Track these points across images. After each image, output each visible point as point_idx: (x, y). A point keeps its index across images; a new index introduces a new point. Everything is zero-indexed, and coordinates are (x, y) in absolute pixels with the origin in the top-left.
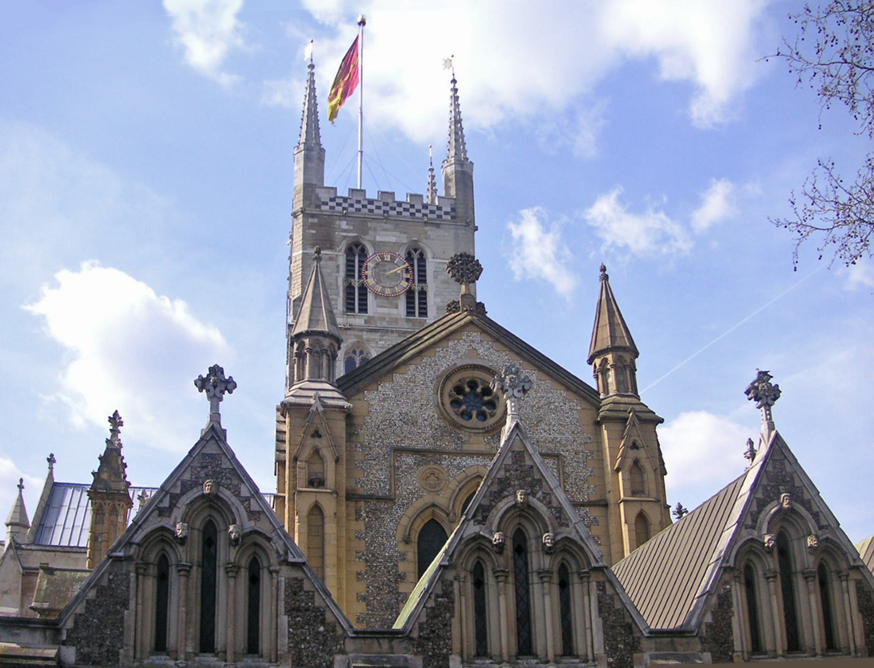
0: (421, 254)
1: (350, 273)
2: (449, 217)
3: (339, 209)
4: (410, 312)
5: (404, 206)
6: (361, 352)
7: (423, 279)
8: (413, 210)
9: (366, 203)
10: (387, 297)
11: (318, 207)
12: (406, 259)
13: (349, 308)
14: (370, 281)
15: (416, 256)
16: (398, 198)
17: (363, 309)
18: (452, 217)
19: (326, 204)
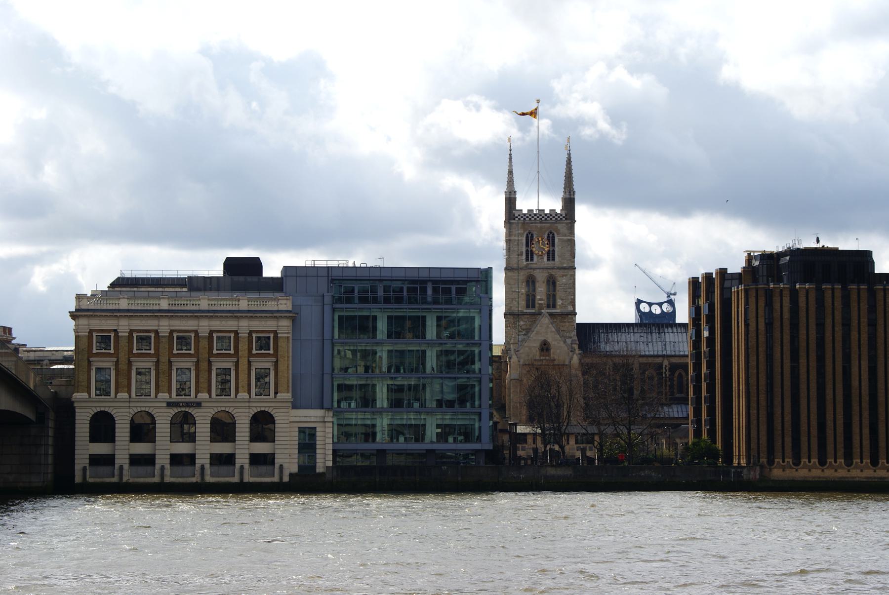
0: (553, 234)
1: (527, 246)
2: (564, 219)
4: (548, 260)
5: (548, 215)
7: (553, 245)
8: (551, 217)
9: (533, 215)
10: (540, 256)
11: (514, 219)
12: (547, 237)
14: (534, 249)
15: (551, 236)
17: (532, 260)
18: (566, 219)
19: (517, 217)
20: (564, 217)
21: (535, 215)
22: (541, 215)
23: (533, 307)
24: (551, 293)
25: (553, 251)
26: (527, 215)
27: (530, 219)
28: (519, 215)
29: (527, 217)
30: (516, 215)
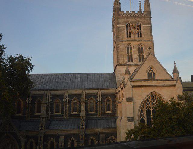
0: (140, 24)
1: (127, 29)
3: (124, 16)
4: (138, 37)
6: (130, 45)
7: (140, 29)
11: (120, 16)
13: (127, 37)
14: (131, 31)
16: (136, 13)
17: (130, 37)
19: (121, 15)
20: (145, 15)
21: (130, 14)
22: (133, 14)
23: (132, 61)
24: (141, 54)
25: (141, 32)
26: (126, 14)
27: (128, 16)
28: (123, 14)
29: (126, 15)
30: (121, 14)
